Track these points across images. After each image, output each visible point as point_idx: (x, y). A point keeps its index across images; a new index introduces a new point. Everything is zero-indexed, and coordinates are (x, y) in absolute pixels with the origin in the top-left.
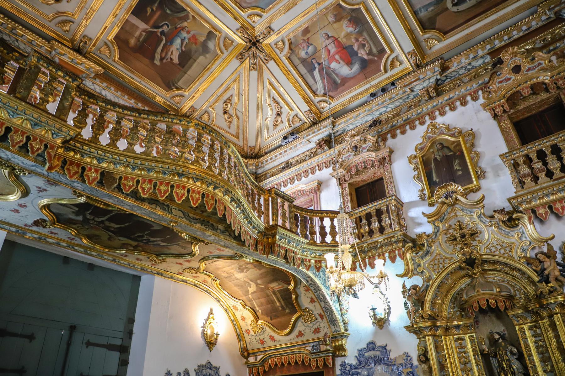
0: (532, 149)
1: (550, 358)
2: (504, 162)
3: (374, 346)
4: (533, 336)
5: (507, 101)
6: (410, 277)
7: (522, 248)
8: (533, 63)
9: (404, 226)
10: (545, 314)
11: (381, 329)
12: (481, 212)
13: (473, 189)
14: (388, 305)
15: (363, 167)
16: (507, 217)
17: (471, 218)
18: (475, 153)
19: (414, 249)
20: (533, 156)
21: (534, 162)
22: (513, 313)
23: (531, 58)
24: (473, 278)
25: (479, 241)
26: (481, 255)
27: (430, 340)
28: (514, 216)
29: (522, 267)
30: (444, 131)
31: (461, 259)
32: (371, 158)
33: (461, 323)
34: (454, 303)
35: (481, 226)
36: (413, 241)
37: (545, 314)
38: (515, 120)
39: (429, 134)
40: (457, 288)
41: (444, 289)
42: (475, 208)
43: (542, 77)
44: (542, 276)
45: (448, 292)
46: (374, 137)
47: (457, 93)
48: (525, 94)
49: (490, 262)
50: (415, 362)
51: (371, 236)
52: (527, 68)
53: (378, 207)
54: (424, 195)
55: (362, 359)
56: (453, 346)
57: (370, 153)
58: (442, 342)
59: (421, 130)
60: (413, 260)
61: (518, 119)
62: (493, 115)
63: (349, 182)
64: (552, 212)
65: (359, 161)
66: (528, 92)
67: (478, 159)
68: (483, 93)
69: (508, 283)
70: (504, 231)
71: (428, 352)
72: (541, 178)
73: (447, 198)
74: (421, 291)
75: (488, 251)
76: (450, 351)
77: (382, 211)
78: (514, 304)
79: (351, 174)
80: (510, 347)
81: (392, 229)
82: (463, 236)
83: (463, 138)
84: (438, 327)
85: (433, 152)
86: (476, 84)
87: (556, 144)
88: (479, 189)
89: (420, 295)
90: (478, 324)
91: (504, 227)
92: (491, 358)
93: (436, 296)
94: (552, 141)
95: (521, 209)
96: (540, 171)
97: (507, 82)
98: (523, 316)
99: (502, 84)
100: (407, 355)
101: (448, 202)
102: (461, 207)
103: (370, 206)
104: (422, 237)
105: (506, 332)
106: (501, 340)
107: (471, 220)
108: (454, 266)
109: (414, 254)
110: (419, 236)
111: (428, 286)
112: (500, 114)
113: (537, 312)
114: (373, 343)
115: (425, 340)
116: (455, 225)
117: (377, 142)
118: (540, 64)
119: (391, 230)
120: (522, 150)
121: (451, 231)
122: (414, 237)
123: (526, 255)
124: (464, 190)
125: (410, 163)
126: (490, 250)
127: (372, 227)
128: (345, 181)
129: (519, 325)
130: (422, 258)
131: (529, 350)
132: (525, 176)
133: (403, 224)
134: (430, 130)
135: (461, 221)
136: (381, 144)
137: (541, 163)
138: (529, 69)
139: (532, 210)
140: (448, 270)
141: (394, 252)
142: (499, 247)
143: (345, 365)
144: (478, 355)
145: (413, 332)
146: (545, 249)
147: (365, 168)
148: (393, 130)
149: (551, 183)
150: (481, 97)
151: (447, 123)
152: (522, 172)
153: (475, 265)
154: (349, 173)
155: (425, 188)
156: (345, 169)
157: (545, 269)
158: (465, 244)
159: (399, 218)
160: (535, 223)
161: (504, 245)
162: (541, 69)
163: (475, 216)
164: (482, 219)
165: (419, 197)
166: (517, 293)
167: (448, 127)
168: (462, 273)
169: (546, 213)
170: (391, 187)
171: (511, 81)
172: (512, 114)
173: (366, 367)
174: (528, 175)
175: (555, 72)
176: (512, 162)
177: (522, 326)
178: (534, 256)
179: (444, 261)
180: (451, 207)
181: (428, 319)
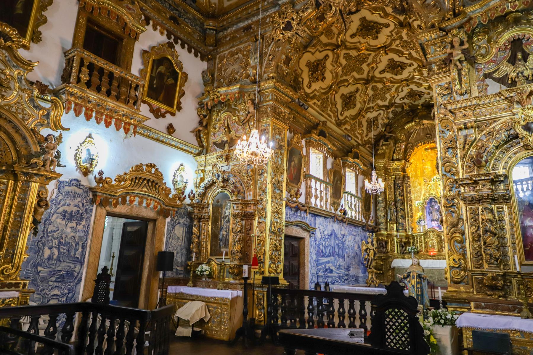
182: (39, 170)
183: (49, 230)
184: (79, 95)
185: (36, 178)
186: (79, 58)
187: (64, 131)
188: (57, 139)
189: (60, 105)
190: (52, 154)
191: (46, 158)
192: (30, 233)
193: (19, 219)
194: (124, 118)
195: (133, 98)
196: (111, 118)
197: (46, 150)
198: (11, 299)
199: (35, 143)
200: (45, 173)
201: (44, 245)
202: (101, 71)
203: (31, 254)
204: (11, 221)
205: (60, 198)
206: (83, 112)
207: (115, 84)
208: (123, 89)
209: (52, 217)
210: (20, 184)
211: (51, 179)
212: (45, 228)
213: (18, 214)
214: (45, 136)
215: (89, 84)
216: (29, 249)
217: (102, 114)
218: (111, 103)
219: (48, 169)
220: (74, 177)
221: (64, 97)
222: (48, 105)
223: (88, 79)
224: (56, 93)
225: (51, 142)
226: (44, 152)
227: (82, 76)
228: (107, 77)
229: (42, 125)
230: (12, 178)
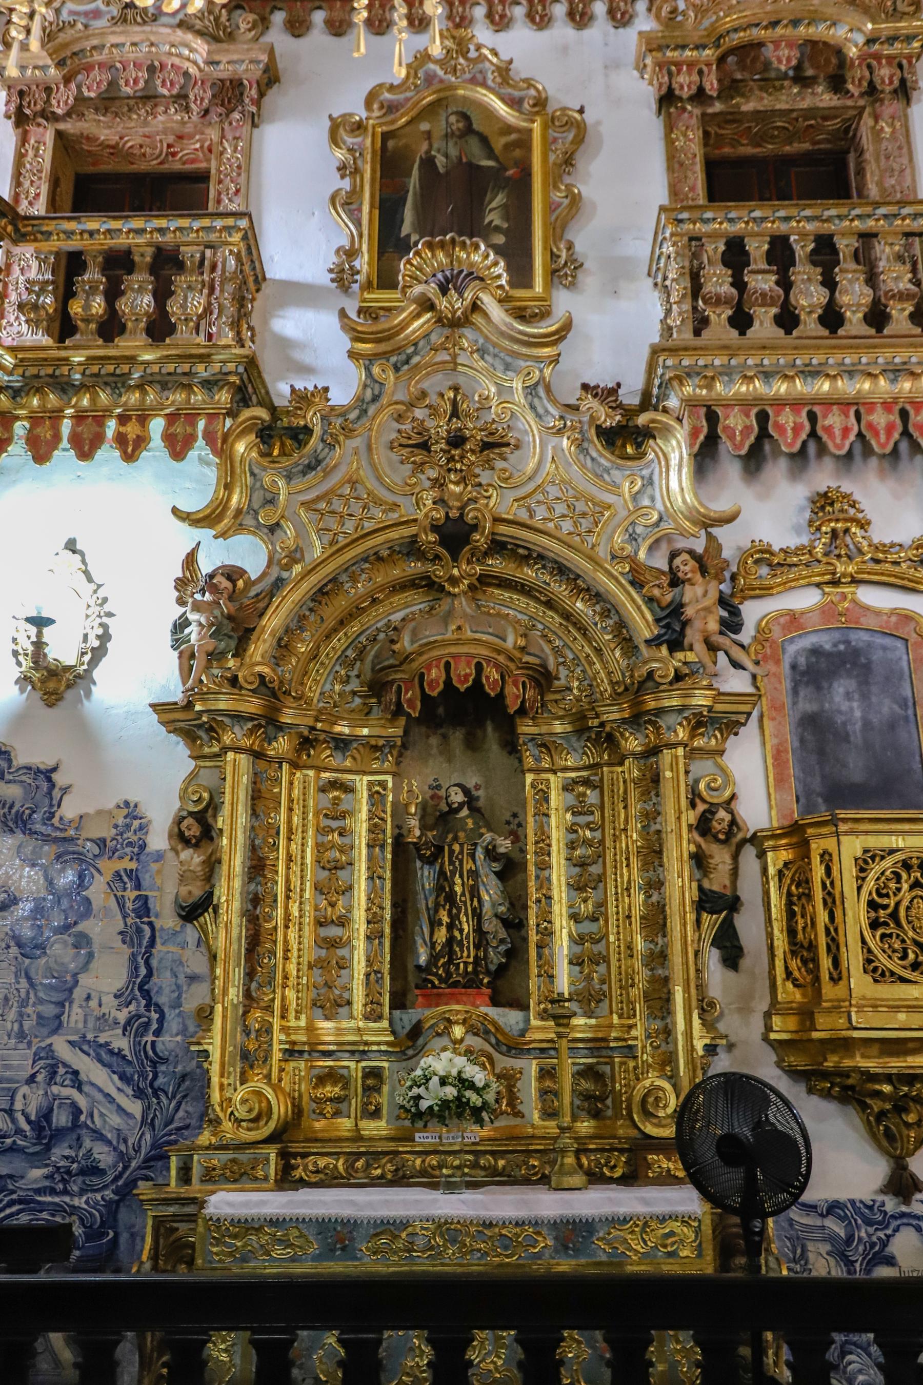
7: (631, 530)
16: (618, 418)
20: (757, 248)
25: (504, 470)
30: (490, 76)
37: (633, 743)
42: (528, 357)
43: (847, 28)
50: (158, 840)
58: (278, 781)
62: (664, 89)
70: (593, 459)
72: (761, 323)
73: (444, 290)
82: (457, 440)
83: (545, 127)
87: (831, 236)
91: (596, 448)
94: (826, 221)
101: (443, 304)
102: (481, 341)
111: (279, 583)
121: (419, 413)
123: (636, 553)
140: (370, 543)
141: (192, 419)
142: (560, 509)
146: (699, 546)
153: (468, 547)
155: (365, 247)
161: (580, 506)
163: (518, 385)
164: (536, 400)
165: (331, 271)
168: (415, 567)
174: (727, 301)
180: (447, 331)
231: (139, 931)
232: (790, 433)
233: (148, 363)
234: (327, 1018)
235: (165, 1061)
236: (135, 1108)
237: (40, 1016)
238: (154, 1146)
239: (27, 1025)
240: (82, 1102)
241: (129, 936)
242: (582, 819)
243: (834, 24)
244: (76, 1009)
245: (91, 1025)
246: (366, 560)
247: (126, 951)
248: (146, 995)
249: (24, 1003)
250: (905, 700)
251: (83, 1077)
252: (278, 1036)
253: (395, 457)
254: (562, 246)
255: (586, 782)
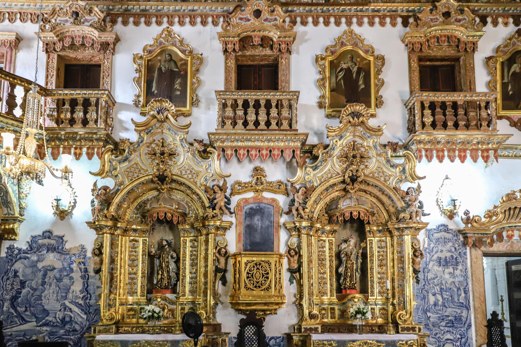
0: (241, 96)
1: (197, 264)
2: (217, 99)
3: (51, 235)
4: (191, 247)
5: (240, 41)
6: (103, 178)
8: (271, 15)
9: (110, 126)
10: (204, 232)
11: (62, 220)
12: (184, 137)
13: (184, 113)
14: (75, 200)
15: (81, 43)
17: (174, 139)
18: (197, 80)
19: (114, 152)
20: (240, 103)
21: (238, 108)
22: (182, 227)
23: (272, 8)
24: (160, 192)
25: (174, 162)
26: (172, 175)
27: (107, 239)
28: (208, 150)
29: (200, 193)
31: (154, 174)
32: (93, 37)
33: (139, 227)
34: (138, 210)
35: (180, 150)
36: (116, 144)
37: (204, 232)
38: (239, 63)
39: (162, 39)
40: (144, 198)
41: (132, 197)
42: (181, 132)
44: (212, 204)
45: (135, 199)
46: (103, 12)
47: (201, 8)
48: (255, 42)
49: (177, 182)
50: (89, 254)
51: (72, 125)
52: (265, 18)
53: (87, 96)
54: (139, 101)
55: (34, 245)
56: (127, 245)
57: (93, 29)
58: (118, 240)
59: (155, 30)
60: (110, 162)
61: (242, 64)
63: (59, 53)
64: (236, 156)
65: (77, 34)
66: (258, 41)
67: (198, 87)
68: (224, 22)
69: (187, 203)
71: (103, 247)
73: (158, 113)
74: (111, 193)
75: (179, 173)
76: (123, 249)
77: (91, 103)
78: (185, 221)
79: (63, 44)
80: (172, 253)
81: (97, 125)
82: (163, 153)
84: (118, 227)
85: (160, 61)
86: (221, 9)
88: (189, 115)
89: (108, 197)
90: (153, 231)
92: (155, 259)
93: (123, 200)
95: (215, 145)
96: (240, 118)
97: (246, 21)
98: (188, 231)
99: (242, 22)
100: (83, 247)
101: (158, 117)
103: (78, 92)
104: (125, 143)
105: (173, 241)
106: (167, 246)
107: (173, 141)
108: (147, 178)
109: (113, 157)
110: (123, 141)
112: (230, 51)
113: (199, 230)
114: (50, 232)
115: (103, 237)
116: (159, 141)
117: (104, 20)
118: (276, 19)
119: (95, 126)
120: (234, 94)
121: (153, 145)
122: (117, 140)
124: (176, 111)
125: (134, 61)
126: (181, 172)
127: (75, 116)
128: (54, 50)
129: (184, 237)
130: (120, 163)
131: (185, 257)
132: (228, 118)
133: (110, 124)
134: (164, 36)
135: (165, 139)
136: (109, 25)
137: (243, 112)
138: (266, 20)
139: (223, 149)
141: (93, 149)
142: (188, 172)
143: (13, 248)
144: (145, 255)
145: (93, 228)
146: (221, 184)
147: (83, 45)
148: (127, 15)
149: (244, 131)
150: (220, 24)
151: (183, 35)
152: (227, 114)
154: (61, 42)
156: (57, 36)
157: (215, 199)
158: (162, 161)
159: (107, 116)
160: (221, 160)
162: (275, 25)
163: (178, 138)
166: (191, 212)
167: (182, 41)
168: (153, 186)
169: (232, 155)
170: (107, 80)
171: (249, 23)
172: (239, 56)
173: (37, 253)
174: (231, 119)
175: (284, 34)
176: (223, 101)
177: (185, 238)
178: (211, 187)
179: (140, 171)
180: (160, 124)
181: (111, 219)
182: (407, 224)
183: (429, 278)
184: (427, 140)
185: (406, 232)
186: (419, 103)
187: (422, 180)
188: (416, 190)
189: (412, 157)
190: (415, 205)
191: (411, 211)
192: (414, 282)
193: (402, 270)
194: (480, 146)
195: (486, 119)
196: (465, 151)
197: (410, 203)
198: (412, 341)
199: (399, 200)
200: (414, 225)
201: (428, 292)
202: (443, 105)
203: (419, 301)
204: (396, 273)
205: (432, 245)
206: (435, 155)
207: (461, 112)
208: (472, 114)
209: (429, 265)
210: (395, 239)
211: (419, 229)
212: (424, 276)
213: (400, 266)
214: (406, 190)
215: (434, 125)
216: (416, 296)
217: (454, 150)
218: (461, 135)
219: (415, 220)
220: (440, 223)
221: (414, 147)
222: (401, 161)
223: (432, 120)
224: (406, 147)
225: (412, 195)
226: (409, 206)
227: (425, 119)
228: (451, 110)
229: (401, 181)
230: (388, 235)
231: (85, 276)
232: (242, 156)
233: (81, 135)
234: (131, 296)
235: (91, 306)
236: (85, 317)
237: (62, 296)
238: (89, 325)
239: (59, 298)
240: (72, 315)
241: (83, 277)
242: (194, 249)
243: (270, 32)
244: (70, 294)
245: (74, 297)
246: (140, 184)
247: (82, 281)
248: (87, 291)
249: (58, 293)
250: (271, 221)
251: (72, 310)
252: (117, 300)
253: (147, 156)
254: (195, 95)
255: (195, 240)
